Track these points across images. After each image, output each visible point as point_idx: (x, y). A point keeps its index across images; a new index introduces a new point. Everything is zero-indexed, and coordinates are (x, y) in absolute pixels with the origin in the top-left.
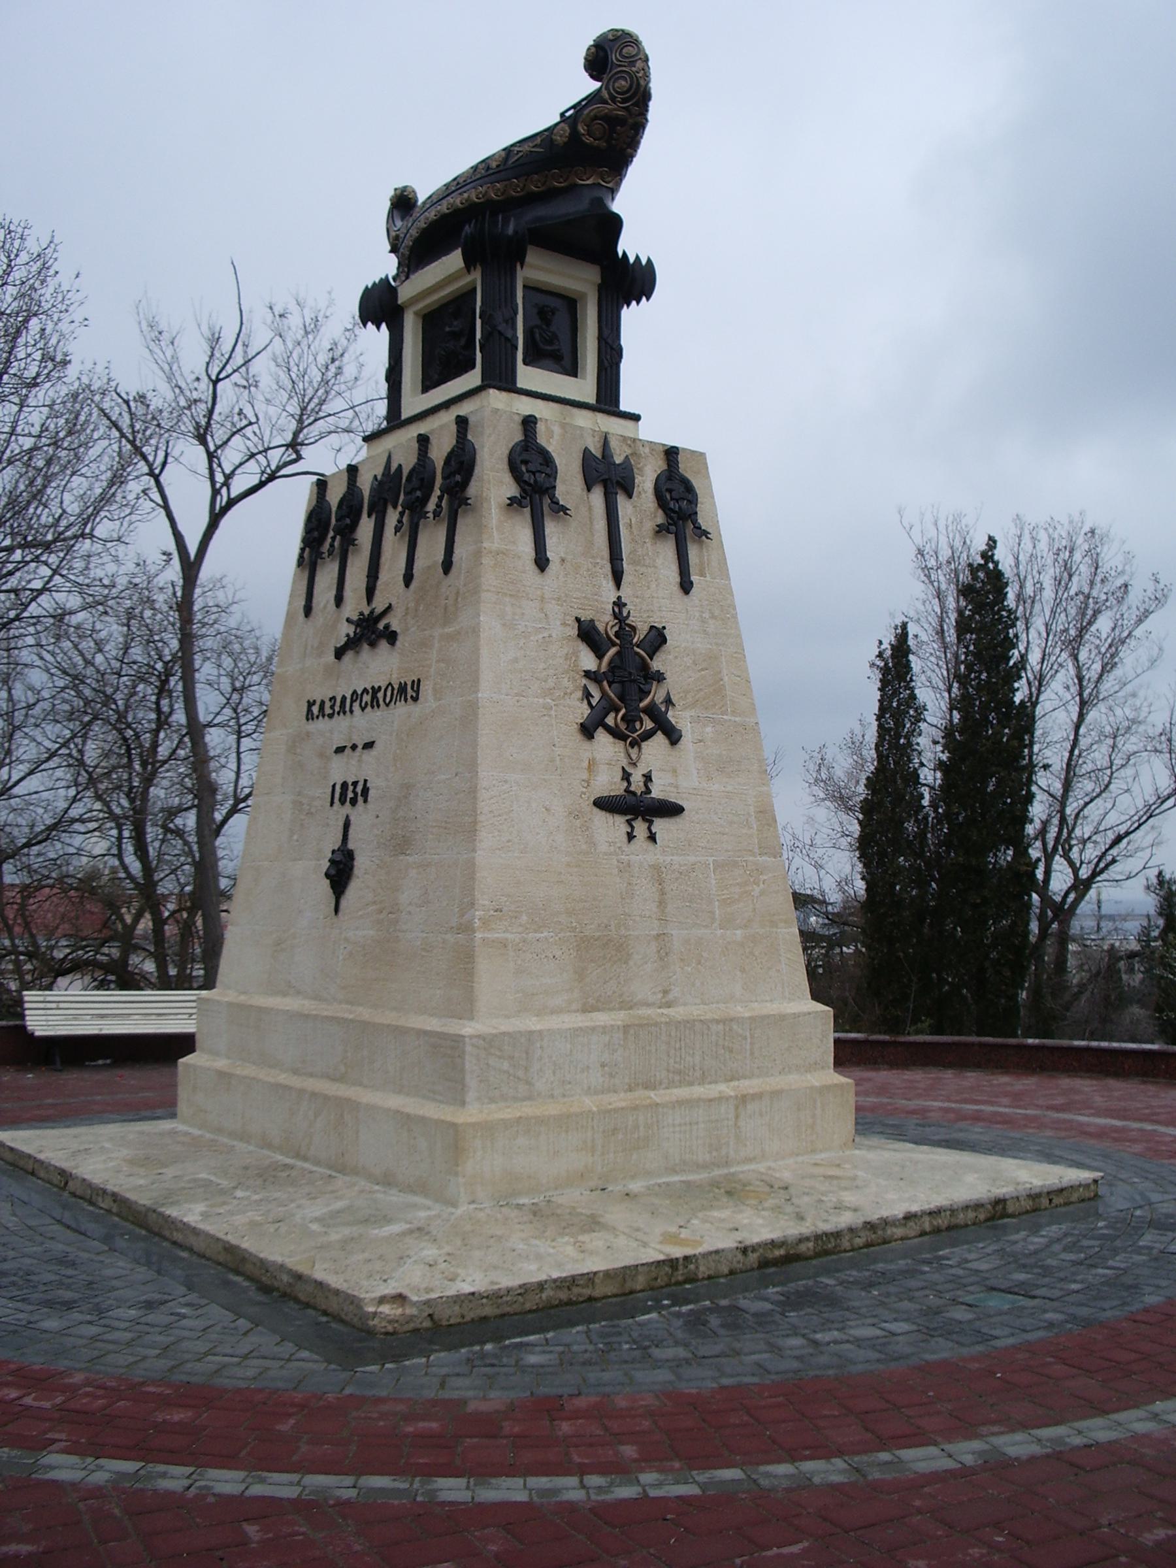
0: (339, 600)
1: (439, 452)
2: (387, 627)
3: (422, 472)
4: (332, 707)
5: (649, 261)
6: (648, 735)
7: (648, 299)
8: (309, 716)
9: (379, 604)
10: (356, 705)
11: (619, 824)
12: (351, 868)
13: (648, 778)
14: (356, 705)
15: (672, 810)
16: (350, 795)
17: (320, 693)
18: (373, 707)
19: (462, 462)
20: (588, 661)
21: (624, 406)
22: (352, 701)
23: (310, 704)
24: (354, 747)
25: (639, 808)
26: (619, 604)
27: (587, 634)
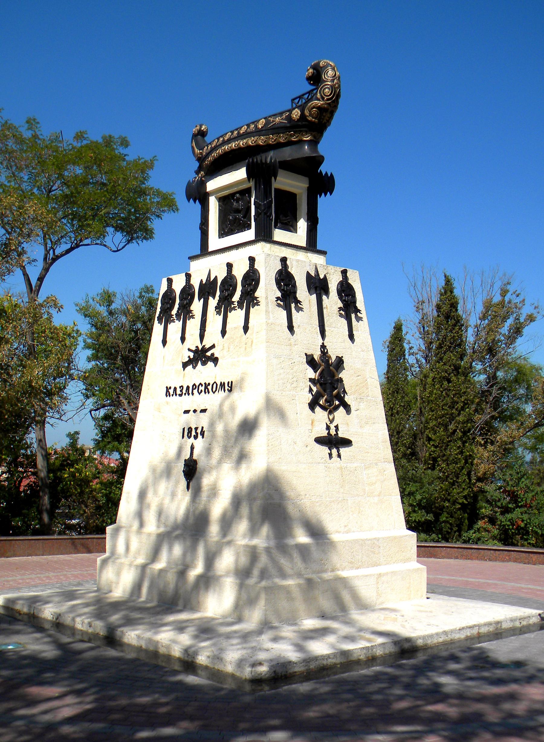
0: (183, 339)
1: (239, 272)
2: (213, 355)
3: (229, 282)
4: (181, 391)
5: (331, 174)
6: (336, 408)
7: (331, 194)
8: (168, 394)
9: (207, 343)
10: (195, 391)
11: (325, 450)
12: (196, 469)
13: (337, 427)
14: (195, 391)
15: (347, 443)
16: (193, 433)
17: (175, 383)
18: (205, 393)
19: (252, 278)
20: (311, 374)
21: (319, 247)
22: (193, 389)
23: (168, 389)
24: (195, 411)
25: (334, 442)
26: (323, 347)
27: (311, 361)
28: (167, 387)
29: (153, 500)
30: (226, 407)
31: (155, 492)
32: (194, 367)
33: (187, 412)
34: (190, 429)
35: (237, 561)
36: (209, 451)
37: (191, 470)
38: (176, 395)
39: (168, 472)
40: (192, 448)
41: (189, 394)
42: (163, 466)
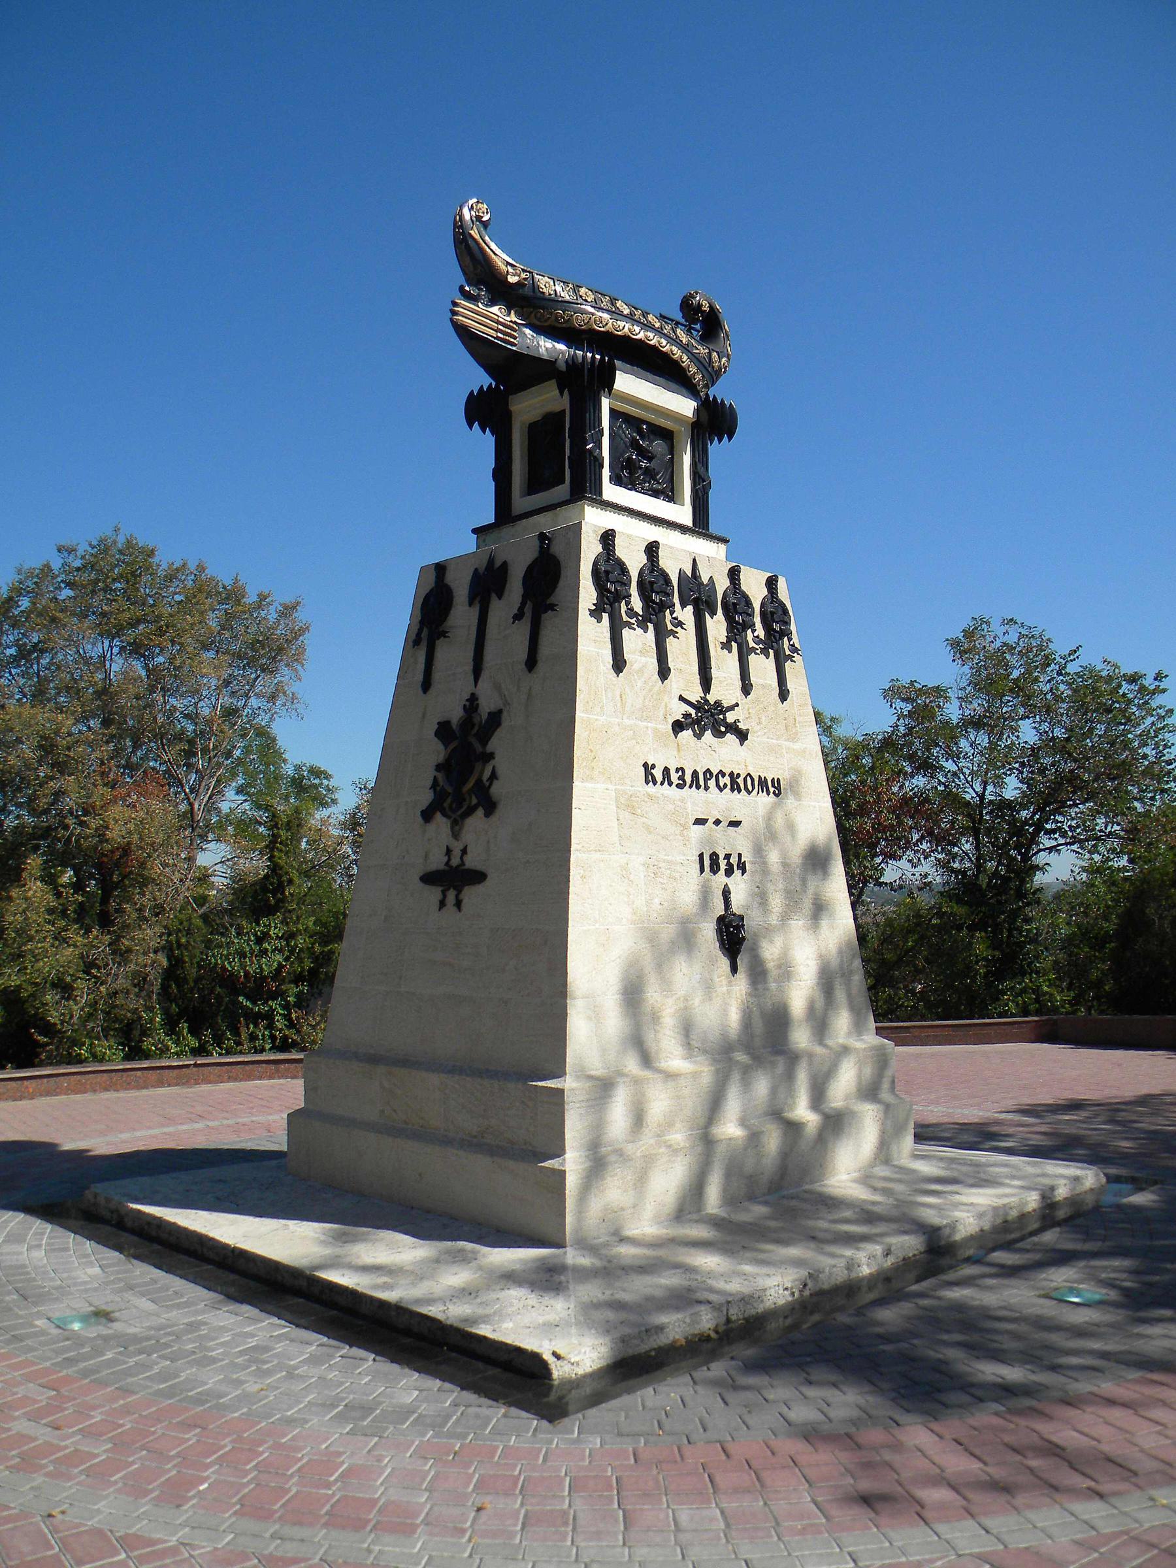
4: (682, 778)
8: (649, 777)
16: (723, 864)
17: (663, 759)
18: (732, 790)
22: (706, 780)
24: (717, 822)
28: (645, 765)
29: (665, 1004)
30: (779, 821)
31: (666, 985)
32: (699, 736)
33: (700, 822)
34: (714, 857)
35: (859, 1076)
36: (761, 897)
37: (732, 936)
38: (670, 784)
39: (686, 939)
40: (726, 893)
41: (698, 787)
42: (669, 932)
